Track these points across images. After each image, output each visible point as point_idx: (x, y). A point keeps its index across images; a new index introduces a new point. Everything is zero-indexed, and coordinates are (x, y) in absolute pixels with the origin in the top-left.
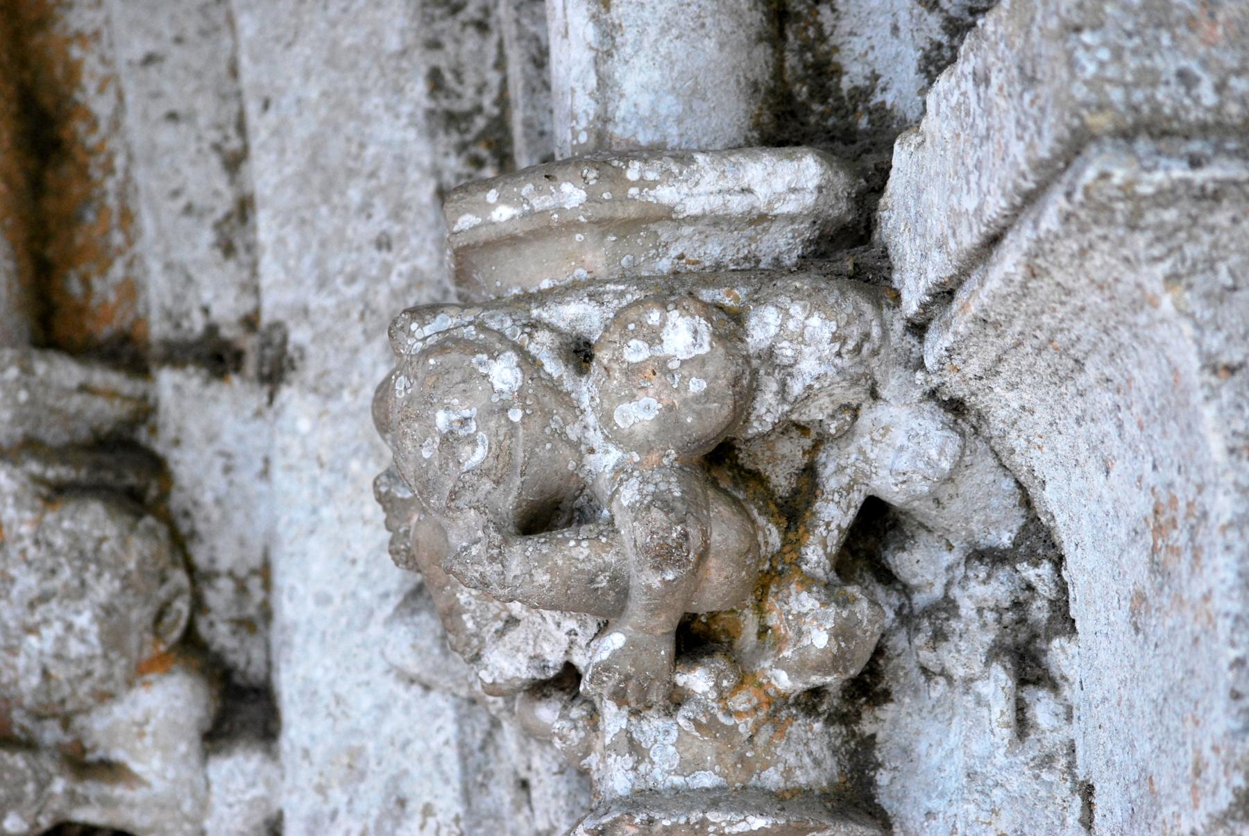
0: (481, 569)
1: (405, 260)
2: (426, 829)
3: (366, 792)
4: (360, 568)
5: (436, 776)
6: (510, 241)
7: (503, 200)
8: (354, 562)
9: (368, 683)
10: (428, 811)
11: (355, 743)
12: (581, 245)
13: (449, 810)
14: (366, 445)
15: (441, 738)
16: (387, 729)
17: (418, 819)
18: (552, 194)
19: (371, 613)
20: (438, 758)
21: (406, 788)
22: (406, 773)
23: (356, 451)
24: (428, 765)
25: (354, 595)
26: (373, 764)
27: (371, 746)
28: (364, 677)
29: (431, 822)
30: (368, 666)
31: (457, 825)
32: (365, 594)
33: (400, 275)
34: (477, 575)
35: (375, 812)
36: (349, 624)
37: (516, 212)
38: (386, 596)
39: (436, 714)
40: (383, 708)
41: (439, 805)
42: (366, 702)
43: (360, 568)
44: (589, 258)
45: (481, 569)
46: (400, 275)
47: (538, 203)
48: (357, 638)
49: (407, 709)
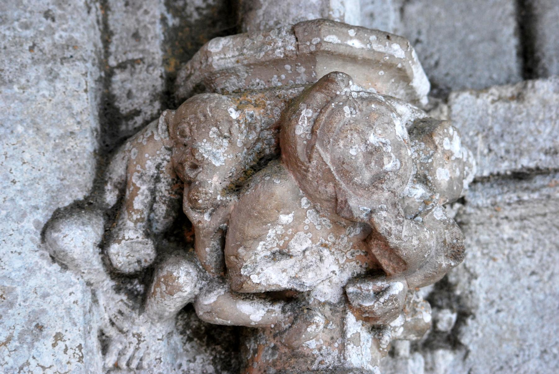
0: (390, 225)
1: (65, 30)
2: (57, 348)
3: (13, 315)
4: (18, 186)
5: (66, 319)
6: (351, 58)
7: (358, 37)
8: (14, 182)
9: (20, 253)
10: (58, 337)
11: (7, 284)
12: (379, 77)
13: (74, 341)
14: (29, 121)
15: (72, 298)
16: (32, 283)
17: (51, 341)
18: (385, 46)
19: (24, 215)
20: (68, 310)
21: (43, 320)
22: (44, 311)
23: (21, 122)
24: (61, 311)
25: (12, 200)
26: (20, 299)
27: (19, 289)
28: (18, 249)
29: (61, 344)
30: (21, 244)
31: (80, 350)
32: (22, 203)
33: (61, 37)
34: (387, 228)
35: (19, 328)
36: (6, 216)
37: (363, 46)
38: (36, 208)
39: (69, 285)
40: (31, 271)
41: (67, 336)
42: (18, 264)
43: (18, 186)
44: (379, 85)
45: (390, 225)
46: (61, 37)
47: (375, 47)
48: (14, 226)
49: (48, 275)
